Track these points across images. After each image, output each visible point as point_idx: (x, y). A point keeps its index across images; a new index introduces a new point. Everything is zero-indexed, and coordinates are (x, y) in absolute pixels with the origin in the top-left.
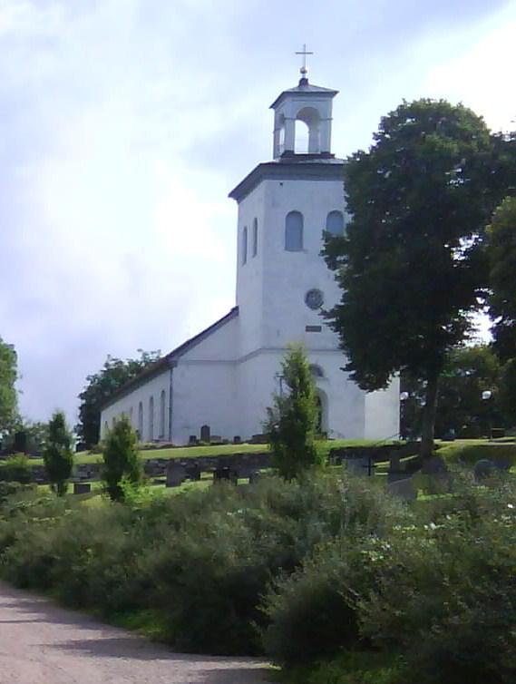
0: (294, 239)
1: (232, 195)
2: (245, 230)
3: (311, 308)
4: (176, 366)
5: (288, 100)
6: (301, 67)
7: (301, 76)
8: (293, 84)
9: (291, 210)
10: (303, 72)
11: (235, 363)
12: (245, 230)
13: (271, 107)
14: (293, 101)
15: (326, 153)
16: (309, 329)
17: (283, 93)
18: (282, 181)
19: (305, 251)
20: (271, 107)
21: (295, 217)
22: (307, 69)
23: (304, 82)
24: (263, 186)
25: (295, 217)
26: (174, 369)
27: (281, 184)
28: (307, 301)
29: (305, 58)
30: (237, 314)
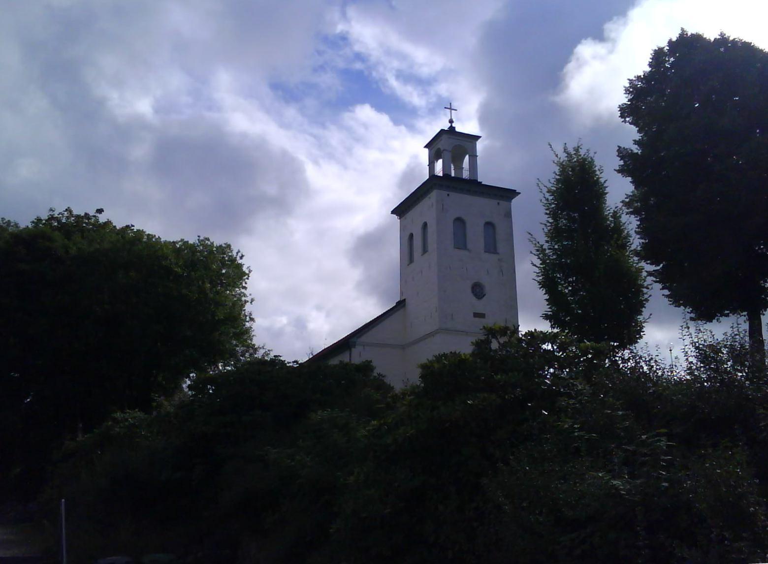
0: (461, 242)
2: (411, 236)
3: (478, 298)
4: (354, 346)
5: (444, 137)
6: (450, 118)
7: (450, 125)
8: (446, 126)
9: (457, 215)
10: (451, 121)
11: (403, 347)
12: (411, 236)
13: (426, 147)
14: (450, 138)
15: (474, 180)
16: (476, 315)
17: (442, 130)
18: (448, 193)
20: (426, 147)
22: (454, 120)
23: (452, 129)
24: (434, 195)
26: (353, 350)
27: (448, 195)
28: (473, 292)
29: (451, 112)
30: (405, 304)
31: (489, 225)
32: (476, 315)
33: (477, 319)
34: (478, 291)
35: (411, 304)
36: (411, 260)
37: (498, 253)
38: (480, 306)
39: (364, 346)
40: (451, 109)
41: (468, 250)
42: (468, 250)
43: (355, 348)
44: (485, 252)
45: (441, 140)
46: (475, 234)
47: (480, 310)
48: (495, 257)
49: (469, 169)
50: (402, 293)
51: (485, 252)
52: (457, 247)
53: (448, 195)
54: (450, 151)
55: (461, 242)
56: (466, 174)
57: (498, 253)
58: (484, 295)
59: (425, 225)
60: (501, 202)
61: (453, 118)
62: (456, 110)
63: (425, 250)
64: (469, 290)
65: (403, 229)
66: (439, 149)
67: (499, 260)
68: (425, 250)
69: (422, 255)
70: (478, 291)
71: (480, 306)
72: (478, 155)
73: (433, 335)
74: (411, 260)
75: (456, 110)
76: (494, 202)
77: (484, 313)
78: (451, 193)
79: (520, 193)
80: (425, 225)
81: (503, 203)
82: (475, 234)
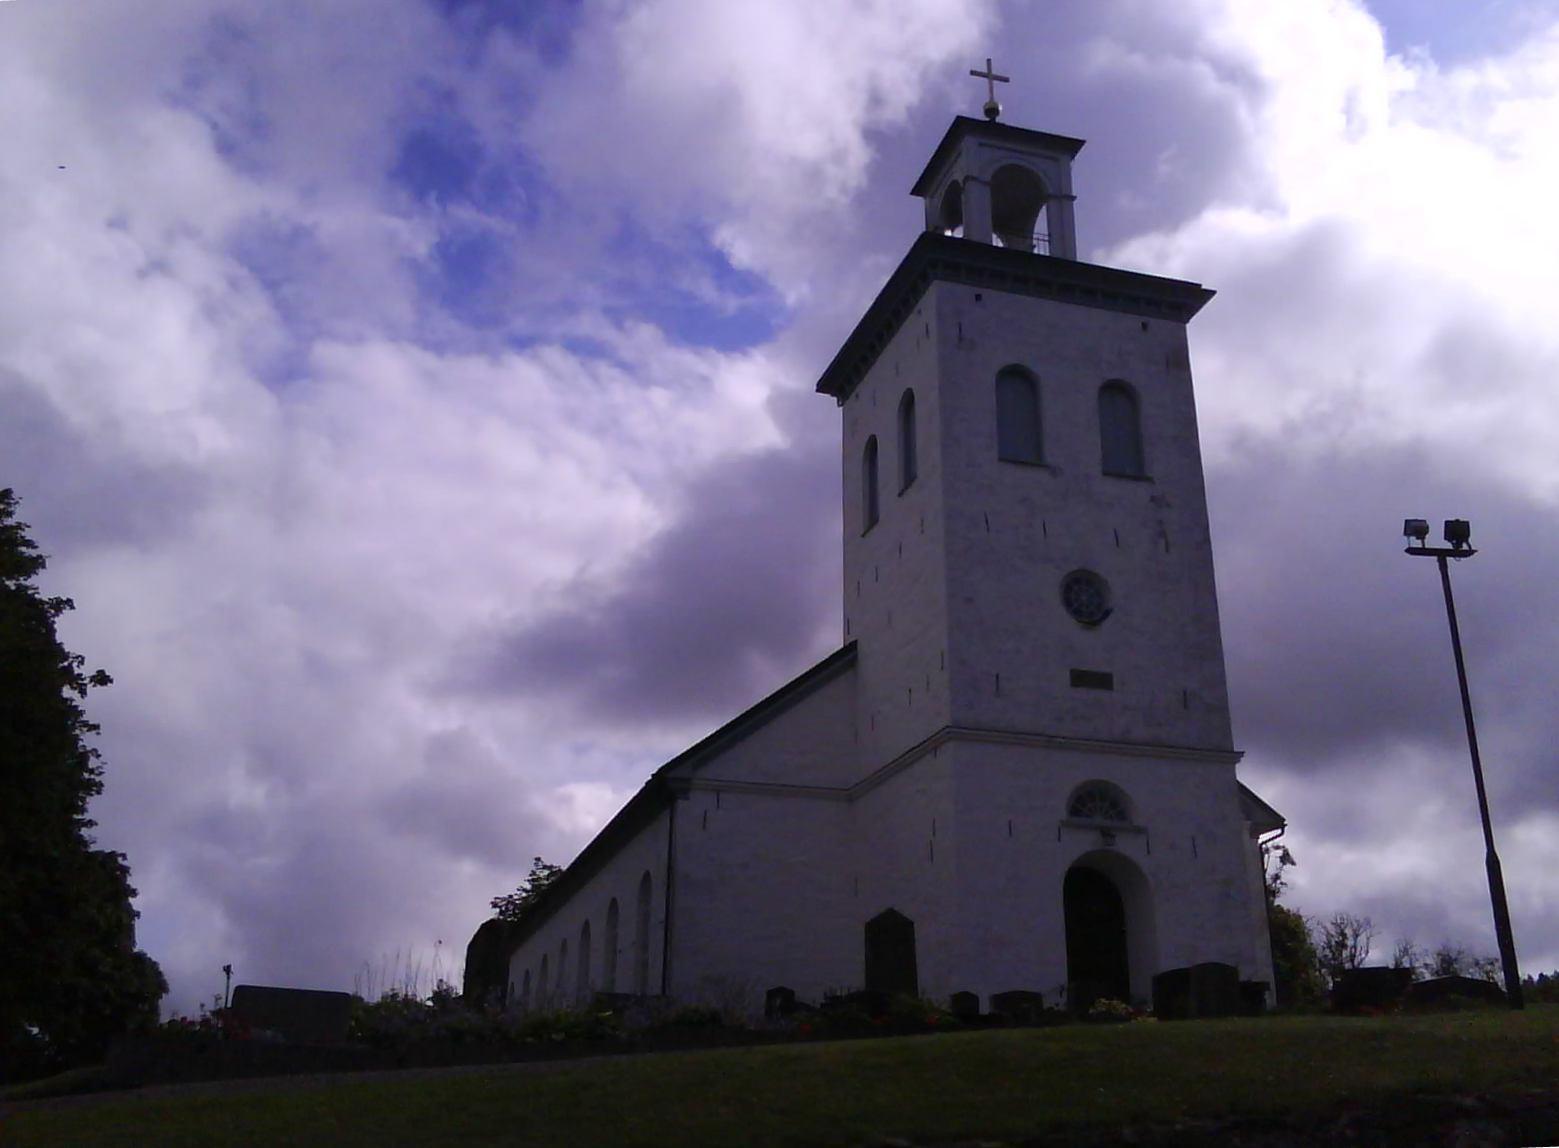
0: (1022, 439)
1: (818, 391)
2: (872, 446)
4: (685, 793)
5: (969, 144)
6: (988, 100)
9: (1011, 360)
11: (849, 795)
12: (872, 446)
13: (914, 192)
14: (981, 145)
16: (1080, 678)
18: (978, 291)
19: (1054, 471)
20: (917, 191)
21: (1017, 379)
24: (932, 298)
25: (1017, 379)
26: (681, 804)
27: (978, 297)
28: (1068, 603)
30: (855, 658)
31: (1117, 392)
32: (1080, 678)
33: (1082, 693)
34: (1084, 596)
35: (869, 662)
36: (873, 519)
37: (1149, 480)
38: (1093, 648)
39: (718, 792)
40: (988, 75)
41: (1046, 467)
42: (1046, 467)
43: (687, 799)
44: (1105, 473)
45: (960, 154)
46: (1071, 418)
47: (1096, 664)
48: (1142, 491)
49: (1050, 235)
50: (847, 630)
51: (1105, 473)
52: (1007, 457)
53: (978, 297)
54: (985, 183)
55: (1022, 439)
56: (1042, 249)
57: (1149, 480)
58: (1107, 613)
59: (908, 402)
60: (1153, 322)
61: (996, 100)
62: (1006, 80)
63: (909, 477)
64: (1053, 596)
65: (850, 427)
66: (955, 182)
67: (1153, 499)
68: (909, 477)
69: (900, 495)
70: (1084, 596)
71: (1093, 648)
72: (1074, 194)
73: (935, 749)
74: (873, 519)
75: (1006, 80)
76: (1131, 322)
77: (1106, 669)
78: (986, 293)
79: (1213, 293)
80: (908, 402)
81: (1160, 326)
82: (1071, 418)
